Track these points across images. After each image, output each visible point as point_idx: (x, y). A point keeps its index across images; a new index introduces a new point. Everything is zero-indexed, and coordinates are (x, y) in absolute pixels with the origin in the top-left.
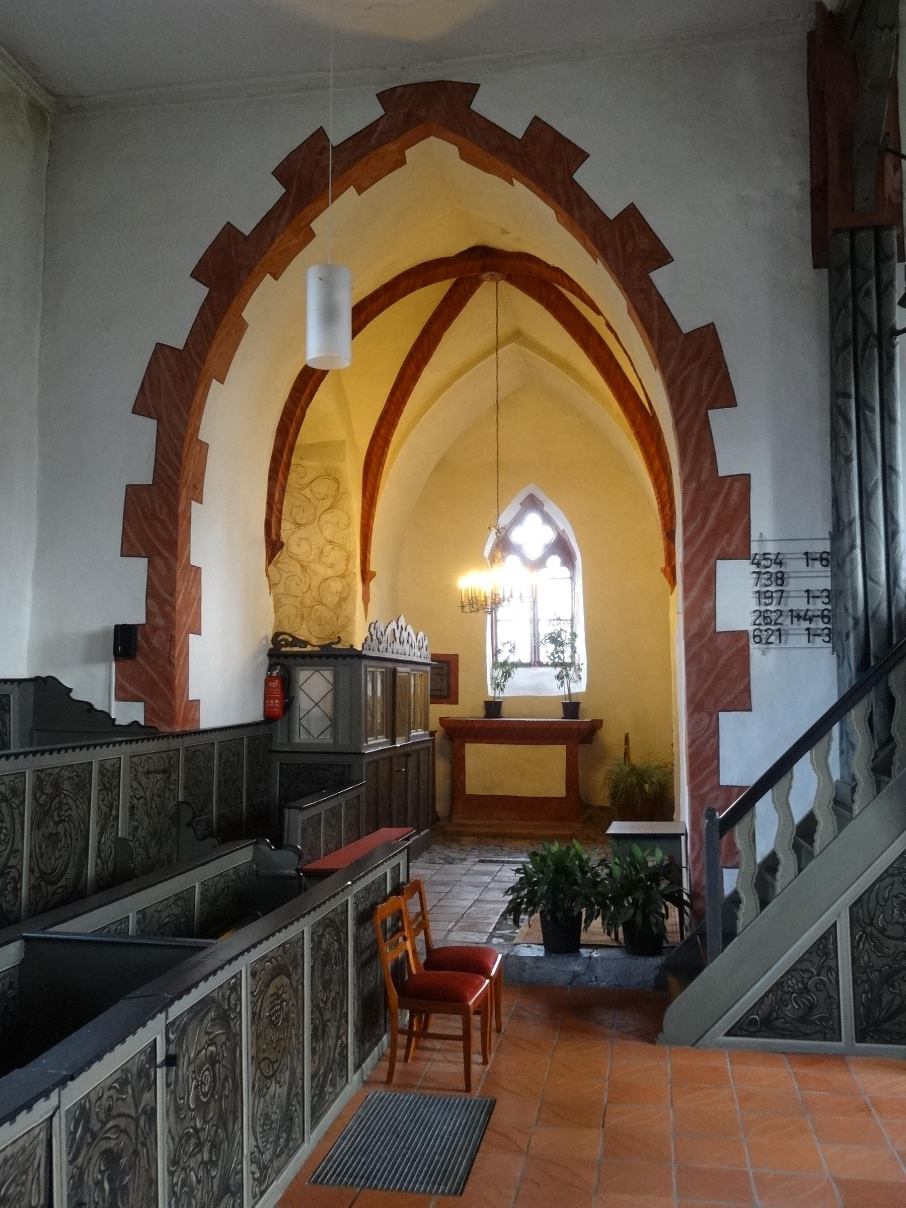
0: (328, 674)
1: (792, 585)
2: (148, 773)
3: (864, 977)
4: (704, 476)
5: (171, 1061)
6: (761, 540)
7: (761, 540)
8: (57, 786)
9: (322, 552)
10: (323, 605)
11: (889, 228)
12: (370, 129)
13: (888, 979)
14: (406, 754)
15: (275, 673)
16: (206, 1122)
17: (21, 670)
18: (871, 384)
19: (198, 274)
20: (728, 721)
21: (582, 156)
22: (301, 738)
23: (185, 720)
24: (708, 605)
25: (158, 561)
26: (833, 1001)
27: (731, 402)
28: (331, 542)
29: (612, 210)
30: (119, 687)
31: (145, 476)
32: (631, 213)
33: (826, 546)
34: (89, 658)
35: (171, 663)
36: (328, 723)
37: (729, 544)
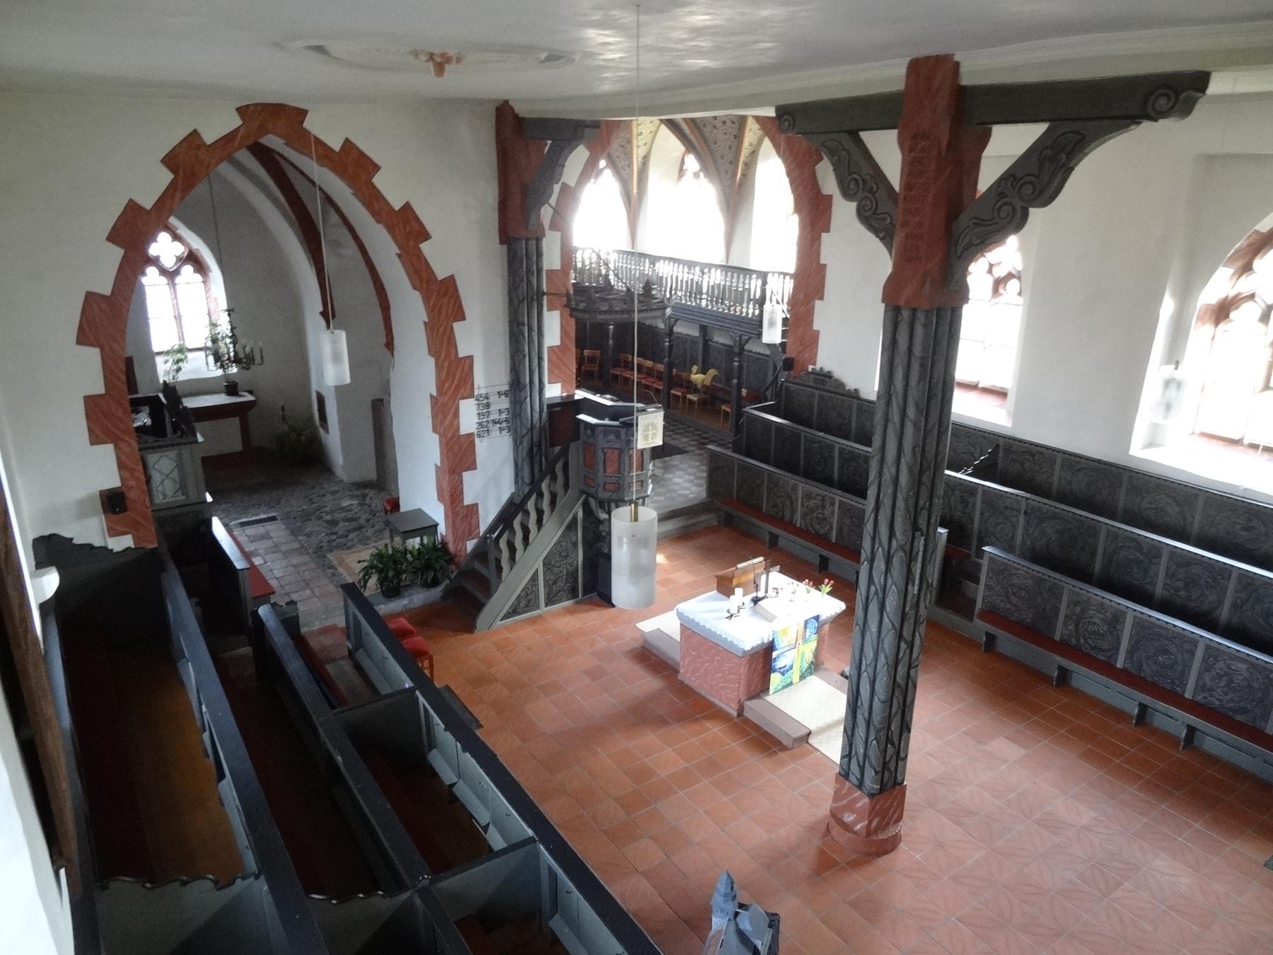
1: (493, 408)
4: (453, 357)
7: (479, 388)
13: (555, 583)
20: (466, 476)
21: (376, 168)
22: (159, 499)
24: (455, 423)
25: (121, 444)
26: (537, 596)
27: (463, 318)
29: (397, 205)
32: (407, 207)
33: (506, 388)
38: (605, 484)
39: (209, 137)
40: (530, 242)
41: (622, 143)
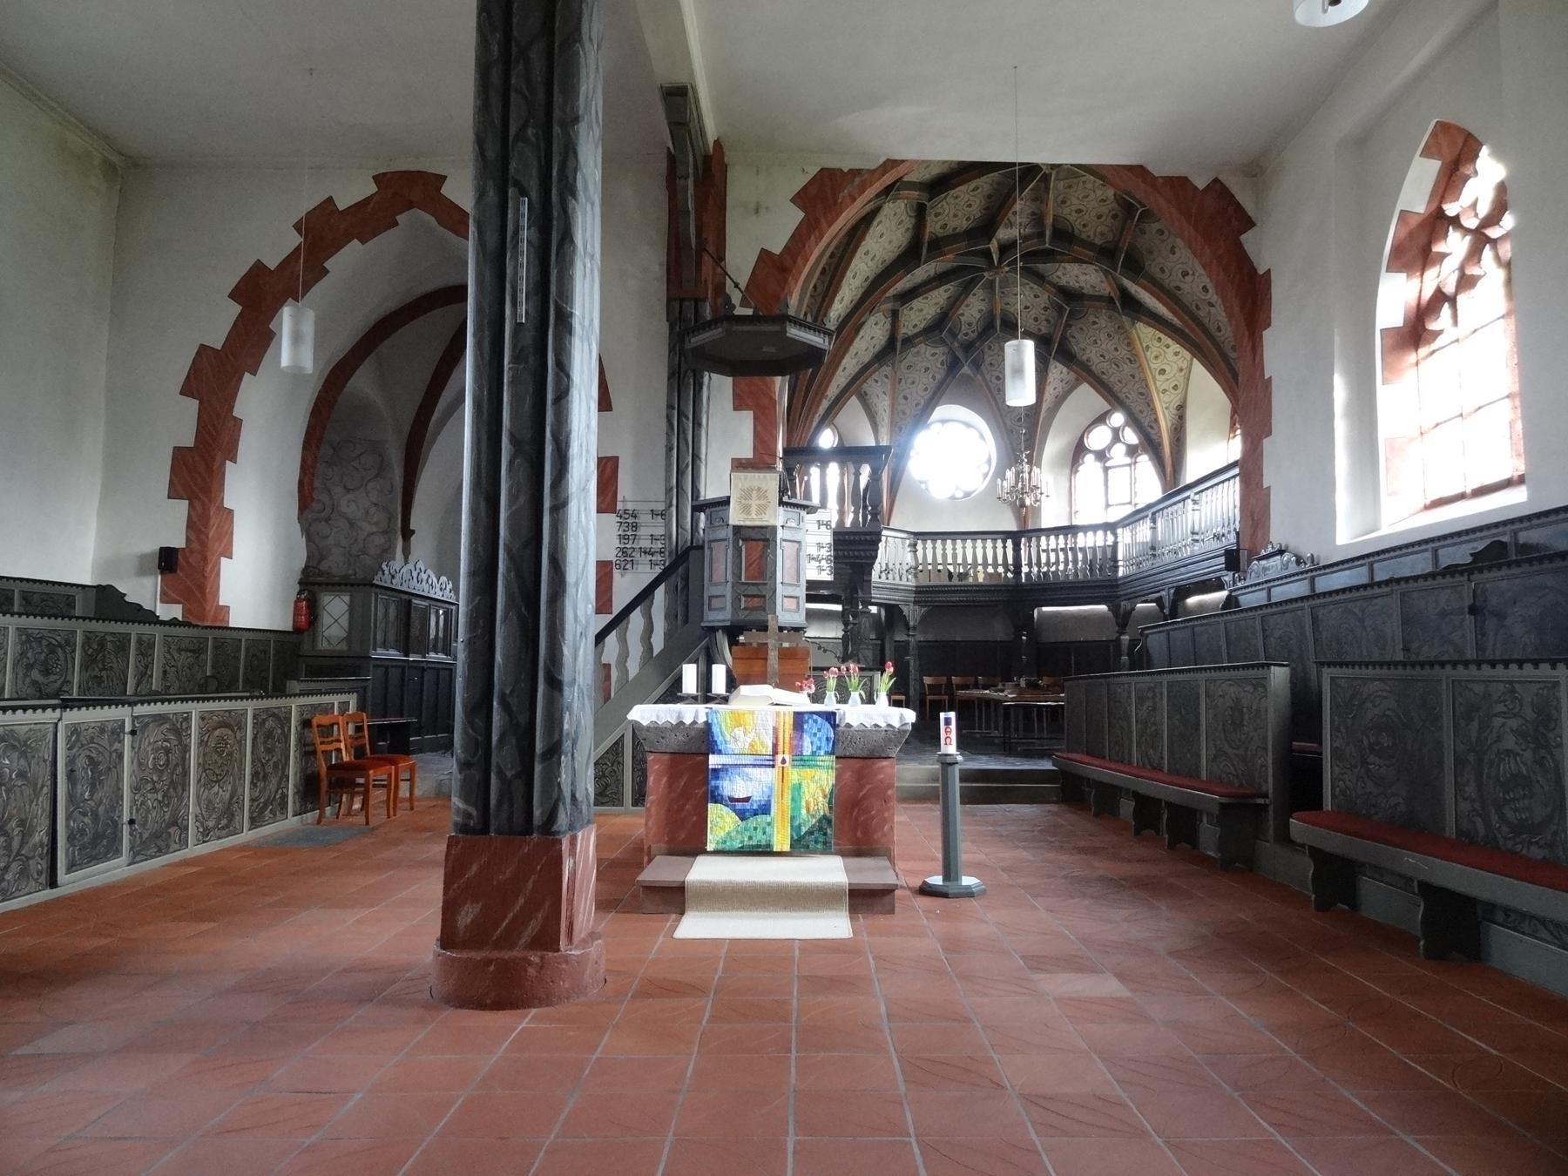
0: (347, 599)
1: (644, 532)
3: (639, 767)
5: (133, 733)
6: (624, 501)
7: (624, 501)
8: (102, 644)
9: (367, 512)
10: (364, 553)
11: (704, 300)
12: (367, 201)
14: (422, 669)
15: (303, 596)
17: (87, 580)
18: (688, 400)
19: (232, 296)
22: (323, 645)
23: (215, 618)
25: (197, 504)
26: (619, 782)
28: (375, 504)
30: (163, 593)
31: (188, 441)
34: (142, 571)
39: (342, 204)
41: (1141, 390)
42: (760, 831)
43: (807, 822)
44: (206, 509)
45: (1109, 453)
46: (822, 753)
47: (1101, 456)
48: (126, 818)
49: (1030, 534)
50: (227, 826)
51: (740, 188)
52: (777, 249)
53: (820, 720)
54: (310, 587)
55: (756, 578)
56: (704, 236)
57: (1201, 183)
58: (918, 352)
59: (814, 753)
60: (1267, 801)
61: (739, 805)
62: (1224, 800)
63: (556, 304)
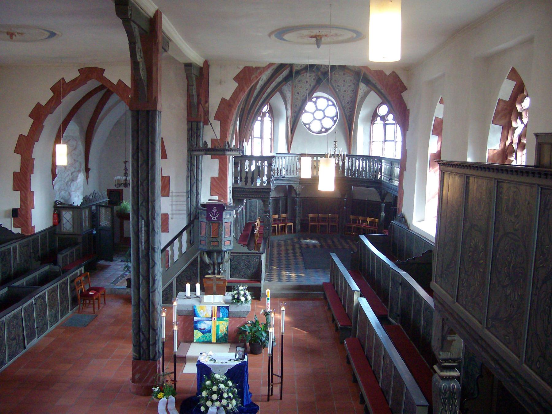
0: (71, 213)
2: (23, 247)
5: (35, 304)
6: (172, 192)
7: (172, 192)
8: (4, 253)
11: (200, 122)
16: (41, 313)
22: (64, 230)
34: (6, 216)
35: (27, 218)
36: (71, 226)
37: (164, 192)
38: (201, 240)
39: (67, 81)
40: (193, 123)
42: (208, 337)
43: (221, 334)
44: (26, 194)
45: (387, 117)
46: (225, 317)
47: (383, 118)
48: (36, 327)
49: (349, 156)
50: (56, 320)
51: (214, 75)
52: (228, 98)
53: (224, 308)
54: (58, 209)
55: (215, 236)
56: (200, 97)
57: (388, 73)
58: (303, 75)
59: (223, 317)
60: (351, 327)
61: (202, 330)
62: (341, 327)
63: (151, 246)
